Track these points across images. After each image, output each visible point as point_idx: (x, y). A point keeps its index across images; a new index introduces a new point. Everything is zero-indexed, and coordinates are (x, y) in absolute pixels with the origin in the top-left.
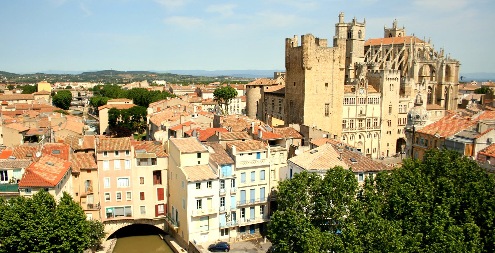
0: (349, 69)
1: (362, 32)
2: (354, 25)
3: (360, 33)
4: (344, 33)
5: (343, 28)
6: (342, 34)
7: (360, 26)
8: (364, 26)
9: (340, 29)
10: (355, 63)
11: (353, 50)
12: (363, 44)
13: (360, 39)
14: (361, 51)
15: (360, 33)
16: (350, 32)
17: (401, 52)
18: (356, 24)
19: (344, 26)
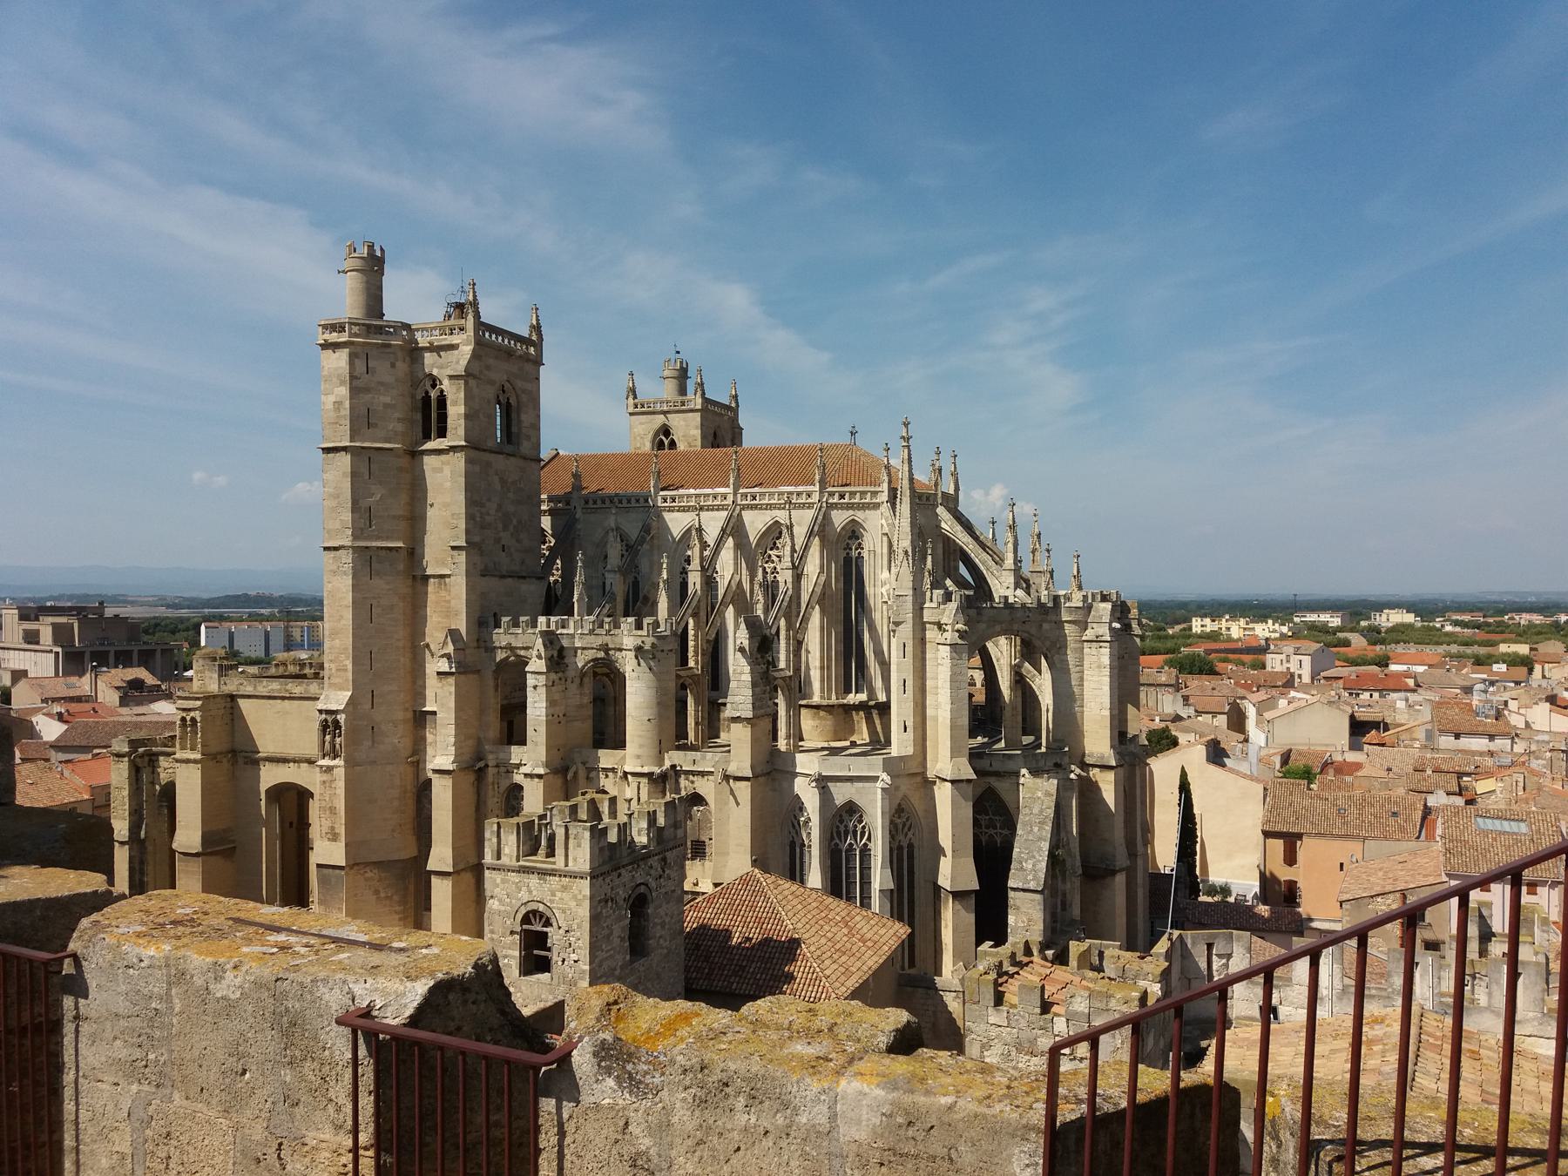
4: (387, 400)
13: (509, 449)
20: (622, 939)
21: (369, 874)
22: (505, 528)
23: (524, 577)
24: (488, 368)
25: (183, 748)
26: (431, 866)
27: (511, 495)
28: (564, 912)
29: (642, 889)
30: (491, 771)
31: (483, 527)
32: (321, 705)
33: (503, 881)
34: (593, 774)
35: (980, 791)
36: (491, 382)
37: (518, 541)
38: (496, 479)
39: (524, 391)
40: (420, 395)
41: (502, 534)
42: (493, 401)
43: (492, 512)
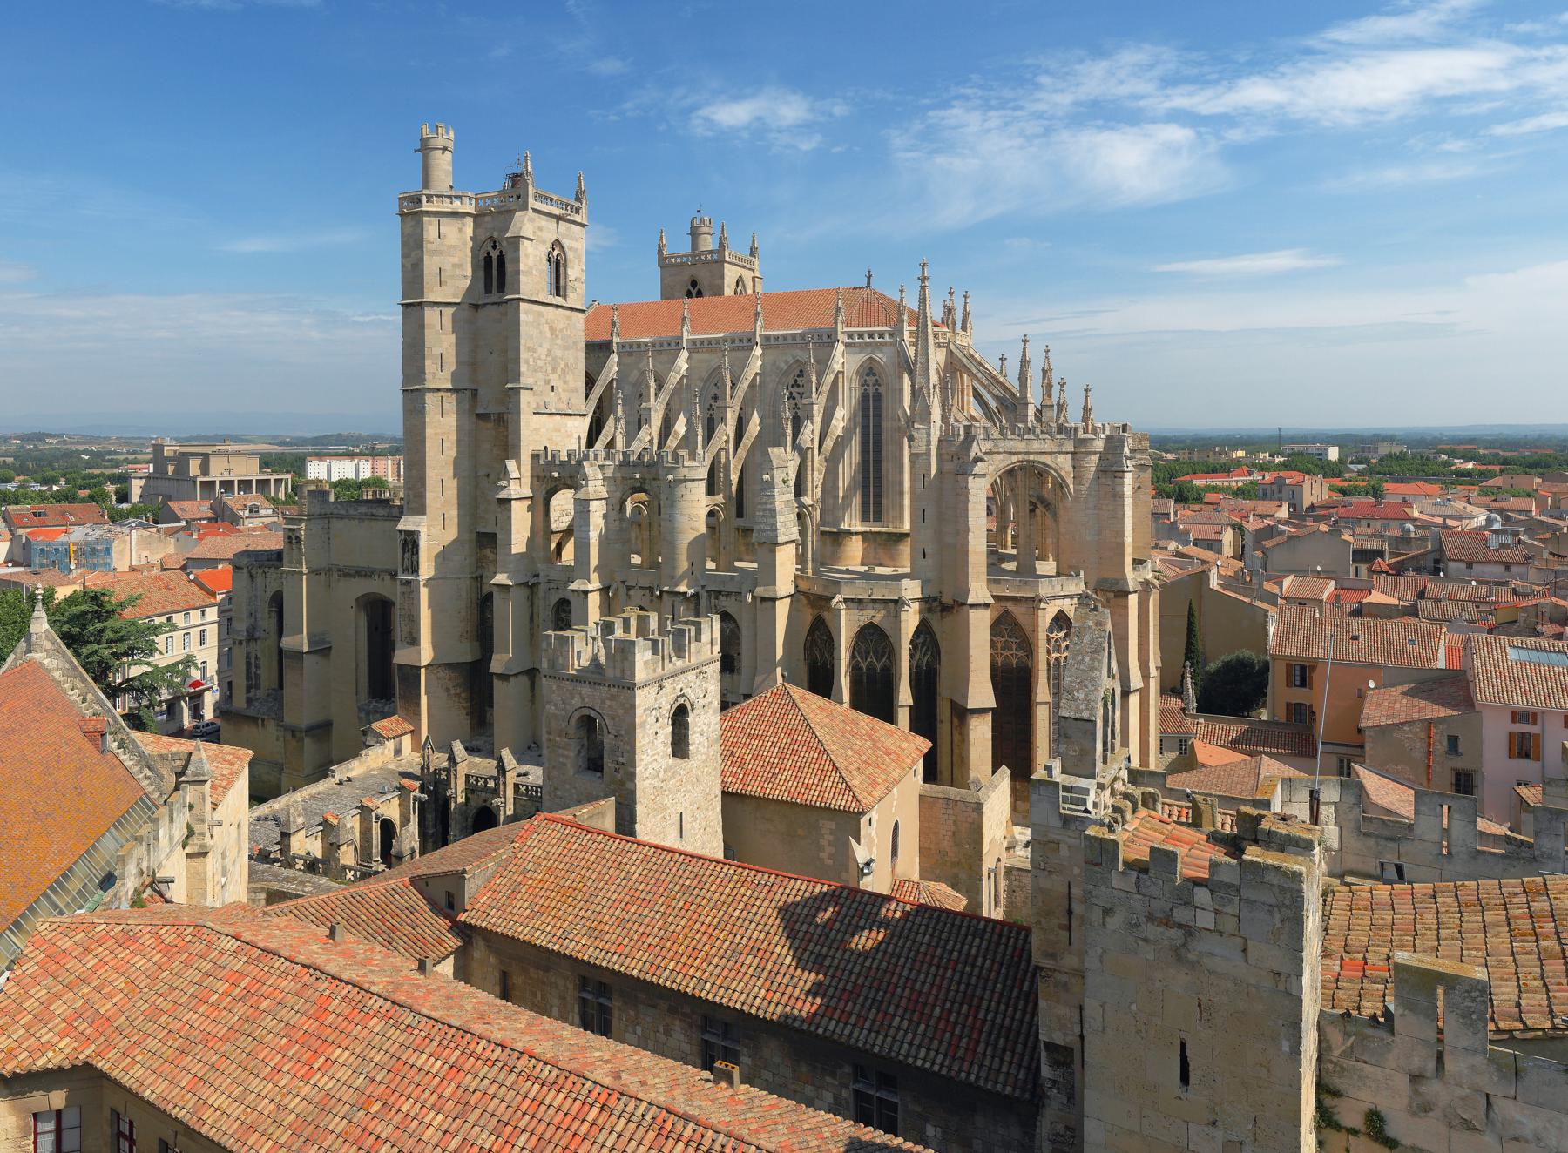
0: (502, 495)
1: (570, 255)
2: (525, 207)
3: (558, 262)
4: (456, 260)
5: (450, 228)
6: (447, 267)
7: (558, 218)
8: (577, 218)
9: (430, 228)
10: (535, 457)
11: (523, 368)
12: (577, 329)
13: (559, 300)
14: (569, 378)
15: (557, 265)
16: (494, 254)
17: (830, 378)
18: (532, 203)
19: (455, 214)
20: (666, 745)
21: (441, 674)
22: (554, 370)
23: (570, 415)
24: (540, 229)
25: (291, 562)
26: (496, 666)
27: (559, 341)
28: (613, 719)
29: (681, 701)
30: (543, 587)
31: (536, 371)
32: (400, 527)
33: (558, 687)
34: (632, 592)
35: (996, 614)
36: (544, 242)
37: (565, 382)
38: (547, 327)
39: (571, 249)
40: (483, 255)
41: (551, 376)
42: (545, 258)
43: (543, 357)
